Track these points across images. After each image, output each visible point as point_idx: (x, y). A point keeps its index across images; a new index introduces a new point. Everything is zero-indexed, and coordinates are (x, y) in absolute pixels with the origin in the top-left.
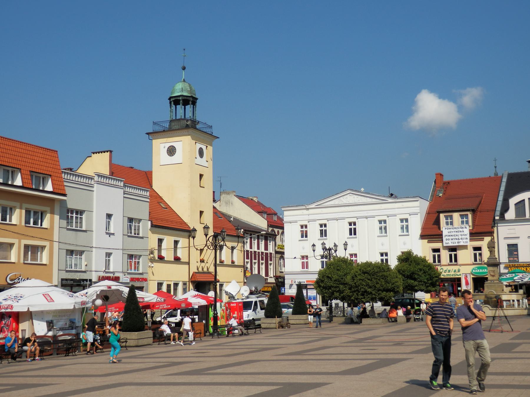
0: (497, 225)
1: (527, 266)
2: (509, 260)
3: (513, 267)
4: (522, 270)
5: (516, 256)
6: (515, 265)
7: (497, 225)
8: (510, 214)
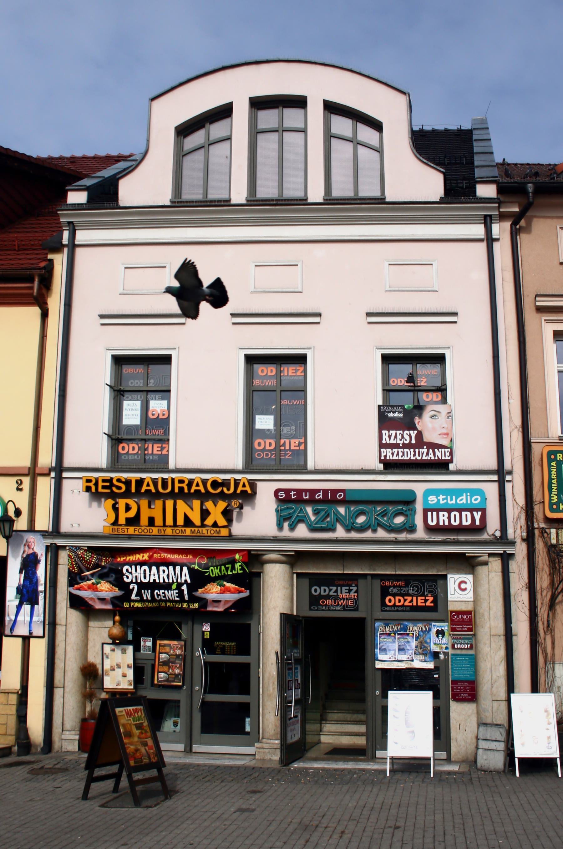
4: (180, 521)
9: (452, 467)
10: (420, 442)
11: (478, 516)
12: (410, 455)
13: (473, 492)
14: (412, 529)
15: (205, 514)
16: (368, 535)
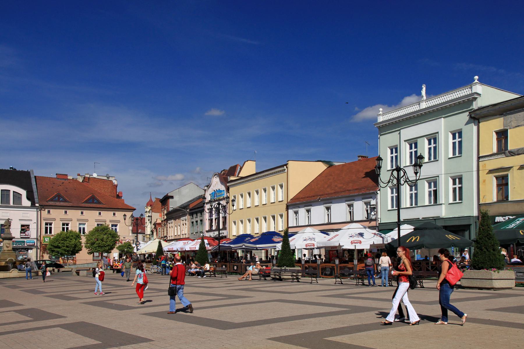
9: (30, 238)
11: (33, 244)
12: (24, 236)
13: (33, 241)
14: (25, 245)
16: (19, 246)
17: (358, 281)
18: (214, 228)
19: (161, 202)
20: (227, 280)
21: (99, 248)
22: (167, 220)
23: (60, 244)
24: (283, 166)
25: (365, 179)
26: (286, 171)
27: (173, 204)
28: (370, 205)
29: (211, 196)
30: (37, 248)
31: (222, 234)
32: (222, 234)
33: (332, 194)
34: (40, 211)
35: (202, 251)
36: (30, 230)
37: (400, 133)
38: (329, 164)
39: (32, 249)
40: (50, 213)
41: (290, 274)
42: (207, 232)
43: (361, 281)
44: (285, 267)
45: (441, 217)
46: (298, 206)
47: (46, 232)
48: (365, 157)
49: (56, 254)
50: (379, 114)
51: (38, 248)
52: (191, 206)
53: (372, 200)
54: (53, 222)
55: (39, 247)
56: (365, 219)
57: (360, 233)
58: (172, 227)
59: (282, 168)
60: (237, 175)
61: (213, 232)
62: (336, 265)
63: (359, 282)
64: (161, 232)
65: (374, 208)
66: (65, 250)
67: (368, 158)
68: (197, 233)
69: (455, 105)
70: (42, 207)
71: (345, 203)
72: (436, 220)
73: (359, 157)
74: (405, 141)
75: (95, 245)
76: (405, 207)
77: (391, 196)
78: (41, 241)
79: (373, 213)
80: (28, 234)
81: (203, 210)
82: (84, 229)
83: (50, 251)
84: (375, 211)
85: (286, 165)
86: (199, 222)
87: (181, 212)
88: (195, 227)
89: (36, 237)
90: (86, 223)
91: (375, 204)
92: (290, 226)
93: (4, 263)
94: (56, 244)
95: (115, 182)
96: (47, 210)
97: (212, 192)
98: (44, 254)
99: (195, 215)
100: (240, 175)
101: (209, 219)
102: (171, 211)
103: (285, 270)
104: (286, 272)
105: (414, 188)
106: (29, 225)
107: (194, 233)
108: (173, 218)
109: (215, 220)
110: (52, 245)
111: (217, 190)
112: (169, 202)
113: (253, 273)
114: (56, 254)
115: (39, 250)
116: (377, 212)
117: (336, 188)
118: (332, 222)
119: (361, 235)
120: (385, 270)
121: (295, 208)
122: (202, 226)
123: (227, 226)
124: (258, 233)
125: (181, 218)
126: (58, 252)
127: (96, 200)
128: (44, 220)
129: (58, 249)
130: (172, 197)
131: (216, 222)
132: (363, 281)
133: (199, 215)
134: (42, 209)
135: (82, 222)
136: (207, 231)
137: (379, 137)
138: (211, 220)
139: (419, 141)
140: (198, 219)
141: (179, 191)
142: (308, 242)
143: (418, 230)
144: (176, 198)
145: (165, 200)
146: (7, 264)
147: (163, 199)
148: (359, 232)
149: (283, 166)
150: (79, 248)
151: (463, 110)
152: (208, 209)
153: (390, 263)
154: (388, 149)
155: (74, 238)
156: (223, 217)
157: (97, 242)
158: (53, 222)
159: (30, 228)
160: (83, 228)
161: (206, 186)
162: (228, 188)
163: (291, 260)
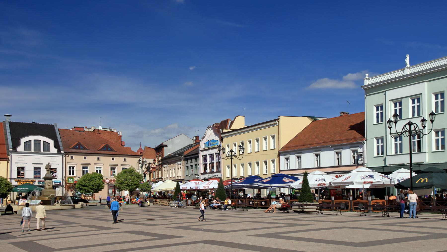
0: (11, 154)
1: (30, 181)
2: (17, 177)
3: (21, 181)
5: (23, 175)
6: (22, 180)
7: (11, 154)
8: (21, 148)
10: (54, 176)
11: (60, 183)
15: (30, 183)
17: (384, 214)
18: (208, 171)
19: (155, 150)
20: (248, 213)
21: (127, 187)
22: (162, 165)
23: (86, 184)
24: (275, 120)
25: (351, 131)
26: (278, 124)
27: (167, 152)
28: (357, 153)
29: (205, 145)
30: (63, 187)
31: (217, 176)
32: (217, 176)
33: (320, 143)
34: (64, 157)
35: (220, 189)
36: (57, 172)
37: (385, 94)
38: (314, 119)
39: (58, 187)
40: (72, 158)
41: (315, 208)
42: (201, 175)
43: (386, 214)
44: (307, 202)
45: (424, 163)
46: (289, 153)
47: (70, 174)
48: (347, 113)
49: (84, 191)
50: (365, 78)
51: (64, 187)
52: (186, 153)
53: (359, 148)
54: (75, 166)
55: (64, 186)
56: (352, 164)
57: (370, 175)
58: (167, 170)
59: (274, 121)
60: (228, 128)
61: (207, 175)
62: (350, 201)
63: (385, 215)
64: (156, 174)
65: (361, 155)
66: (90, 188)
67: (349, 114)
68: (192, 175)
69: (438, 71)
70: (67, 154)
71: (313, 153)
72: (421, 165)
73: (341, 113)
74: (390, 100)
75: (124, 184)
76: (390, 154)
77: (377, 146)
78: (66, 181)
79: (360, 159)
80: (56, 176)
81: (198, 157)
82: (100, 171)
83: (79, 189)
84: (362, 158)
85: (278, 120)
86: (194, 166)
87: (175, 158)
88: (190, 170)
89: (62, 178)
90: (102, 167)
91: (362, 152)
92: (281, 169)
93: (47, 198)
94: (83, 184)
95: (120, 134)
96: (70, 156)
97: (207, 142)
98: (68, 192)
99: (189, 161)
100: (233, 127)
101: (203, 164)
102: (166, 157)
103: (307, 205)
104: (307, 206)
105: (398, 139)
106: (56, 168)
107: (189, 175)
108: (168, 163)
109: (210, 164)
110: (80, 184)
111: (211, 140)
112: (164, 150)
113: (277, 207)
114: (84, 191)
115: (64, 188)
116: (364, 158)
117: (324, 139)
118: (321, 166)
119: (372, 176)
120: (414, 205)
121: (286, 155)
122: (188, 171)
123: (221, 169)
124: (229, 177)
125: (176, 163)
126: (85, 190)
127: (109, 148)
128: (68, 164)
129: (85, 188)
130: (166, 146)
131: (210, 166)
132: (388, 214)
133: (194, 160)
134: (66, 155)
135: (99, 166)
136: (202, 174)
137: (365, 97)
138: (205, 165)
139: (404, 101)
140: (193, 164)
141: (172, 141)
142: (320, 182)
143: (424, 173)
144: (169, 147)
145: (160, 149)
146: (50, 199)
147: (157, 148)
148: (369, 175)
149: (275, 120)
150: (102, 187)
151: (445, 75)
152: (203, 156)
153: (417, 198)
154: (374, 107)
155: (98, 179)
156: (217, 163)
157: (126, 182)
158: (75, 166)
159: (57, 170)
160: (99, 171)
161: (195, 137)
162: (221, 138)
163: (311, 196)
